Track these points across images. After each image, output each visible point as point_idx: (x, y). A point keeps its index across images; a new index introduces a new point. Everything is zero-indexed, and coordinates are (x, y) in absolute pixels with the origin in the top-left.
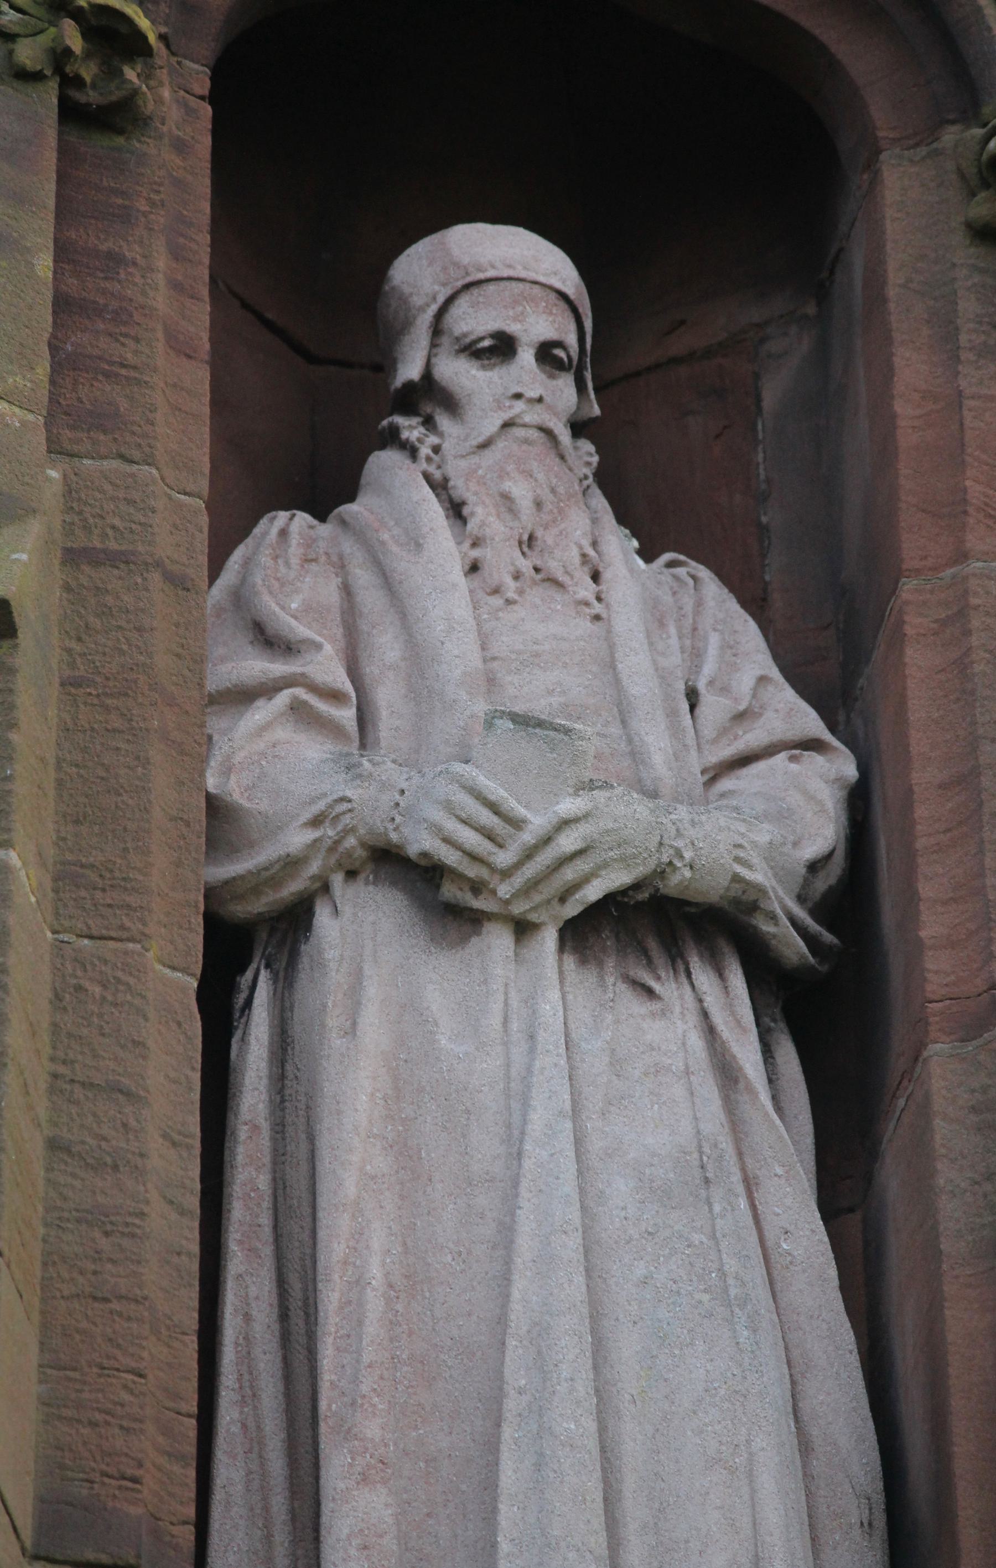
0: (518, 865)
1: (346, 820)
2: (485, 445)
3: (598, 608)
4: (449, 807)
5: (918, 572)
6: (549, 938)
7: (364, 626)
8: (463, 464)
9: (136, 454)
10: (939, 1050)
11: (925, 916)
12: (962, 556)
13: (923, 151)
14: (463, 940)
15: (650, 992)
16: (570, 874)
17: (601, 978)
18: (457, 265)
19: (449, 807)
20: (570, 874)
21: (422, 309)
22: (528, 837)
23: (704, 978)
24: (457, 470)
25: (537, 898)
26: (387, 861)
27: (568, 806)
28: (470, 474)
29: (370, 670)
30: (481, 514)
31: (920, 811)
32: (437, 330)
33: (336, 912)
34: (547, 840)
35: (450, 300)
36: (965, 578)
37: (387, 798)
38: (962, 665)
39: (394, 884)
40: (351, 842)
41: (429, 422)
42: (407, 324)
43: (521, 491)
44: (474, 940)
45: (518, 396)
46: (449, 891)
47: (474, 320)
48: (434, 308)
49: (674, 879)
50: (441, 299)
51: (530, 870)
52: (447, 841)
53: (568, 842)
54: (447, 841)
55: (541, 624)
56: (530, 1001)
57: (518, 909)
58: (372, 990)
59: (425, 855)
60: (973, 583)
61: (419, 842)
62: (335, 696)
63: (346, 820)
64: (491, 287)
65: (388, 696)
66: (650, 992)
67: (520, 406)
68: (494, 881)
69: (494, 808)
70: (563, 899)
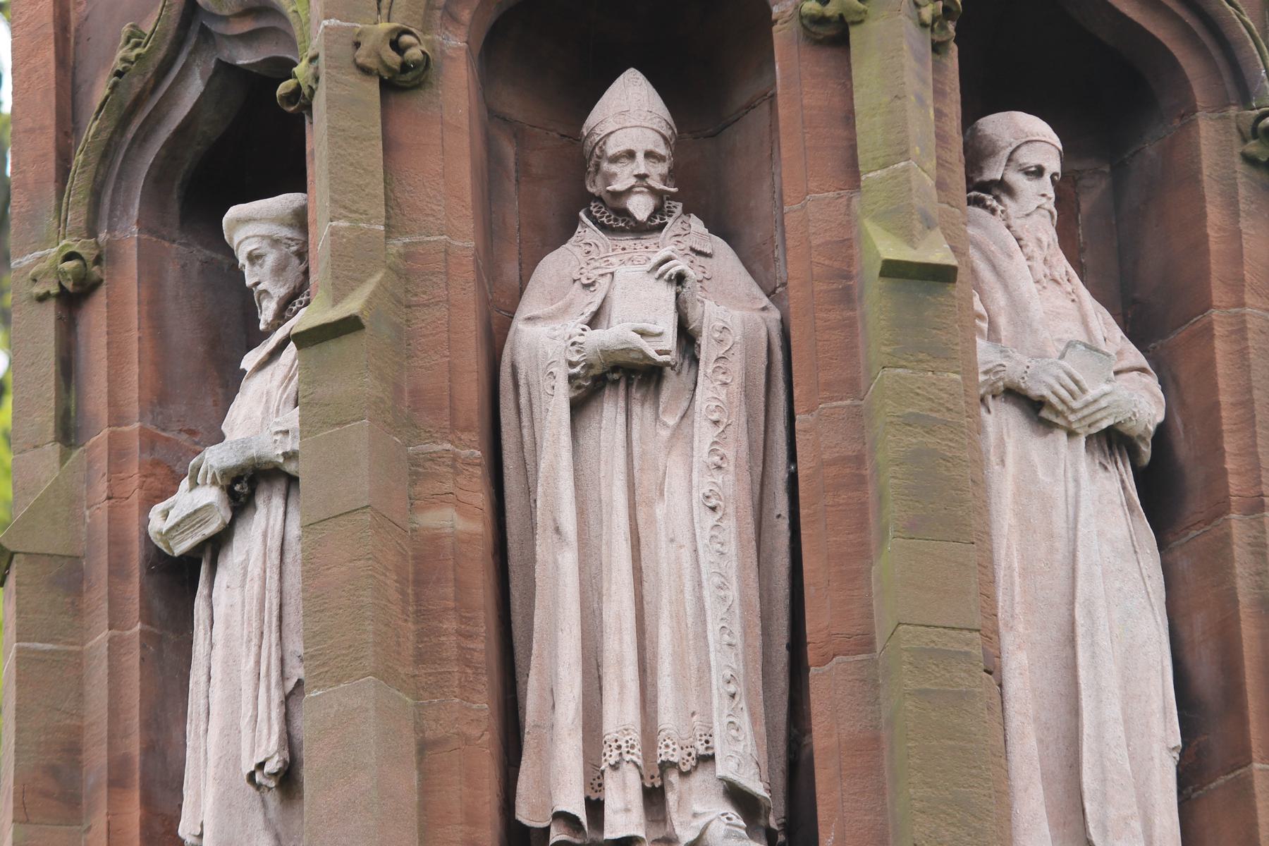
0: (1082, 409)
1: (1002, 374)
2: (1028, 215)
3: (1074, 297)
4: (1058, 378)
5: (1219, 307)
6: (1082, 440)
7: (986, 287)
8: (1019, 222)
9: (954, 203)
10: (1234, 516)
11: (1228, 459)
12: (1243, 305)
13: (1217, 115)
14: (1046, 434)
15: (1106, 468)
16: (1098, 416)
17: (1093, 459)
18: (1022, 131)
19: (1058, 378)
20: (1098, 416)
21: (1003, 148)
22: (1089, 397)
23: (1120, 464)
24: (1016, 223)
25: (1083, 423)
26: (1014, 394)
27: (1107, 388)
28: (1022, 226)
29: (993, 308)
30: (1031, 247)
31: (1224, 414)
32: (1010, 159)
33: (989, 411)
34: (1095, 401)
35: (1018, 147)
36: (1244, 315)
37: (1021, 369)
38: (1243, 353)
39: (1014, 404)
40: (1001, 383)
41: (997, 198)
42: (993, 153)
43: (1045, 239)
44: (1050, 435)
45: (1043, 195)
46: (1045, 414)
47: (1029, 157)
48: (1010, 149)
49: (1129, 425)
50: (1014, 146)
51: (1086, 412)
52: (1054, 393)
53: (1103, 403)
54: (1054, 393)
55: (1057, 299)
56: (1075, 465)
57: (1074, 426)
58: (1010, 448)
59: (1042, 396)
60: (1248, 318)
61: (1037, 389)
62: (980, 317)
63: (1002, 374)
64: (1038, 144)
65: (1002, 321)
66: (1106, 468)
67: (1044, 200)
68: (1067, 413)
69: (1076, 382)
70: (1090, 426)
